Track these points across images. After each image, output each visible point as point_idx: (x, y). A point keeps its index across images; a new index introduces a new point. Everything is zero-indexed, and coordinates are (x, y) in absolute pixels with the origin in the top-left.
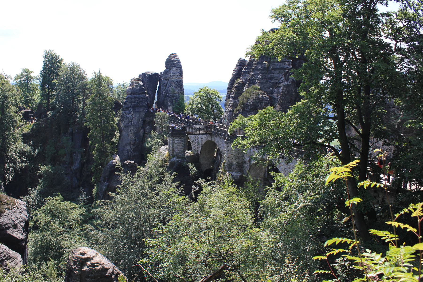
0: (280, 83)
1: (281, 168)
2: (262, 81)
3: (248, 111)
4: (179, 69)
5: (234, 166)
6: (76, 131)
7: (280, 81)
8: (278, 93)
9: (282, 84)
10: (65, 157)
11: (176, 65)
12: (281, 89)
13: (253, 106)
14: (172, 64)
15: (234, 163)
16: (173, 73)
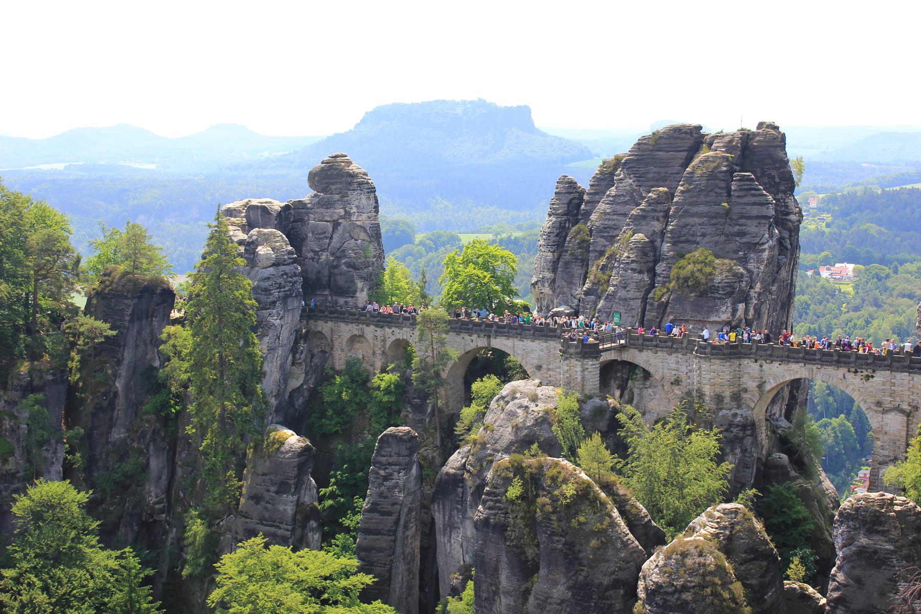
0: (763, 244)
1: (851, 387)
2: (717, 238)
3: (719, 299)
4: (372, 195)
5: (727, 400)
6: (50, 377)
7: (763, 240)
8: (759, 261)
9: (766, 246)
10: (10, 459)
11: (366, 186)
12: (766, 255)
13: (729, 289)
14: (350, 184)
15: (727, 394)
16: (358, 207)
